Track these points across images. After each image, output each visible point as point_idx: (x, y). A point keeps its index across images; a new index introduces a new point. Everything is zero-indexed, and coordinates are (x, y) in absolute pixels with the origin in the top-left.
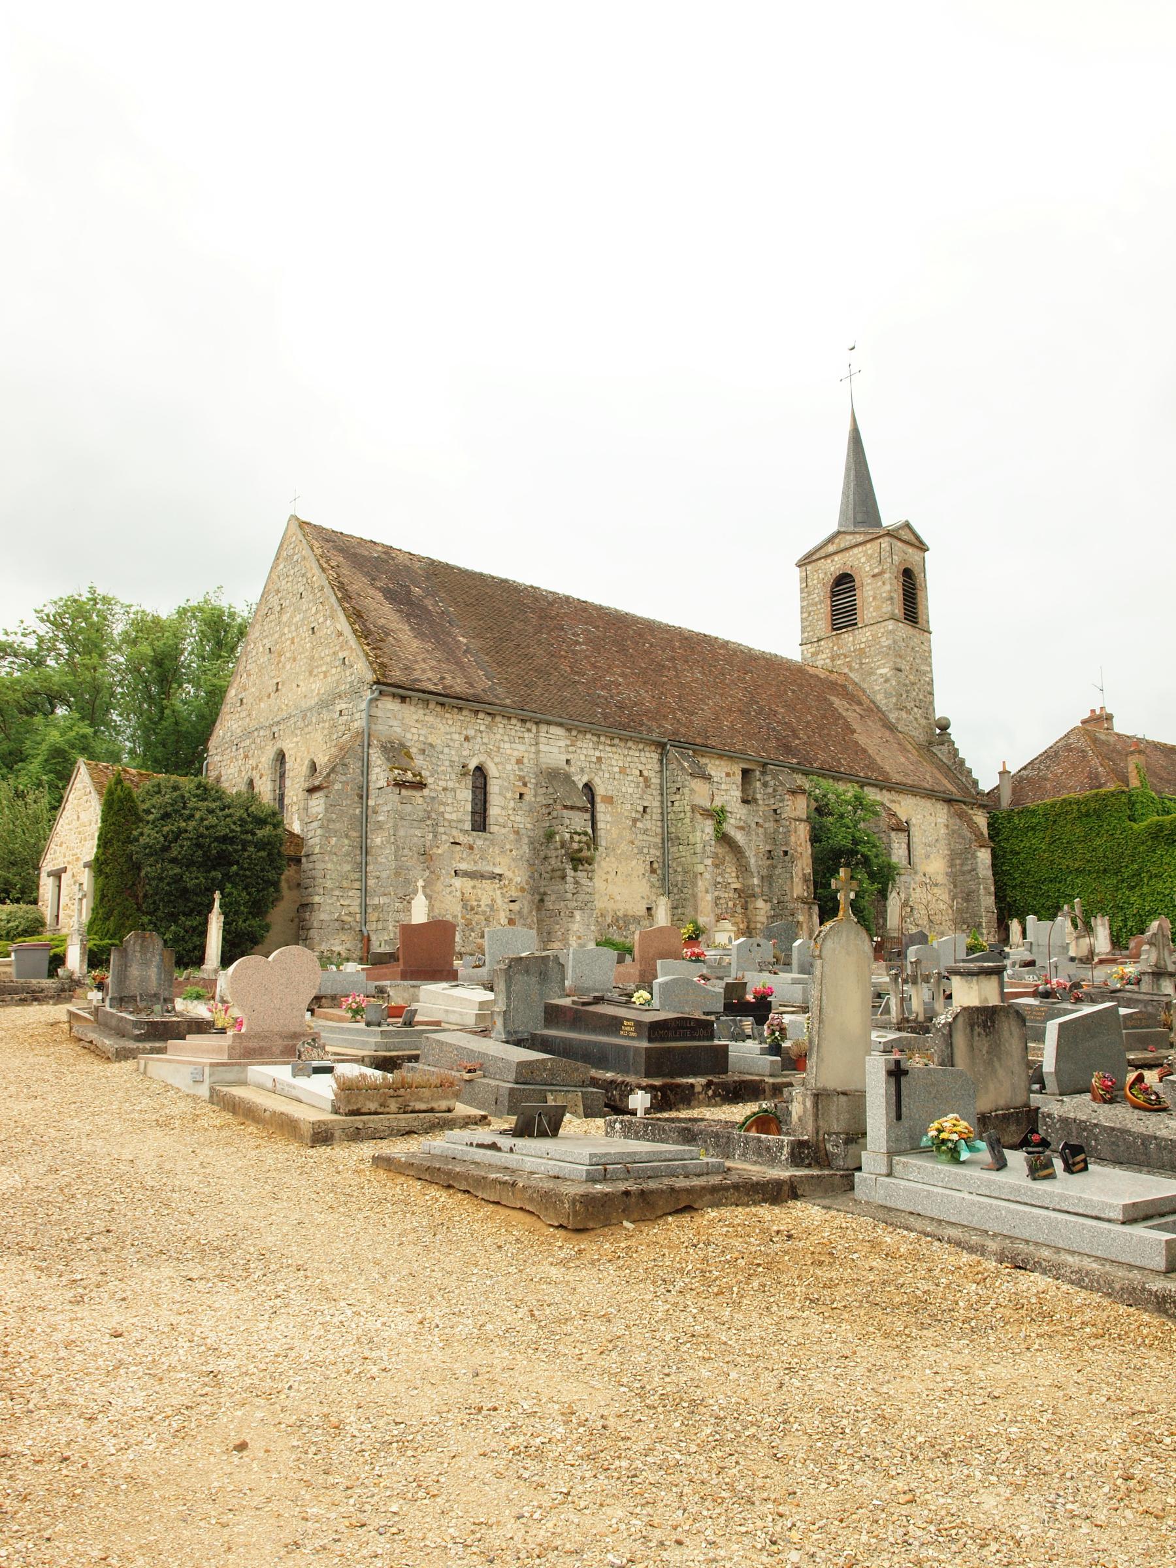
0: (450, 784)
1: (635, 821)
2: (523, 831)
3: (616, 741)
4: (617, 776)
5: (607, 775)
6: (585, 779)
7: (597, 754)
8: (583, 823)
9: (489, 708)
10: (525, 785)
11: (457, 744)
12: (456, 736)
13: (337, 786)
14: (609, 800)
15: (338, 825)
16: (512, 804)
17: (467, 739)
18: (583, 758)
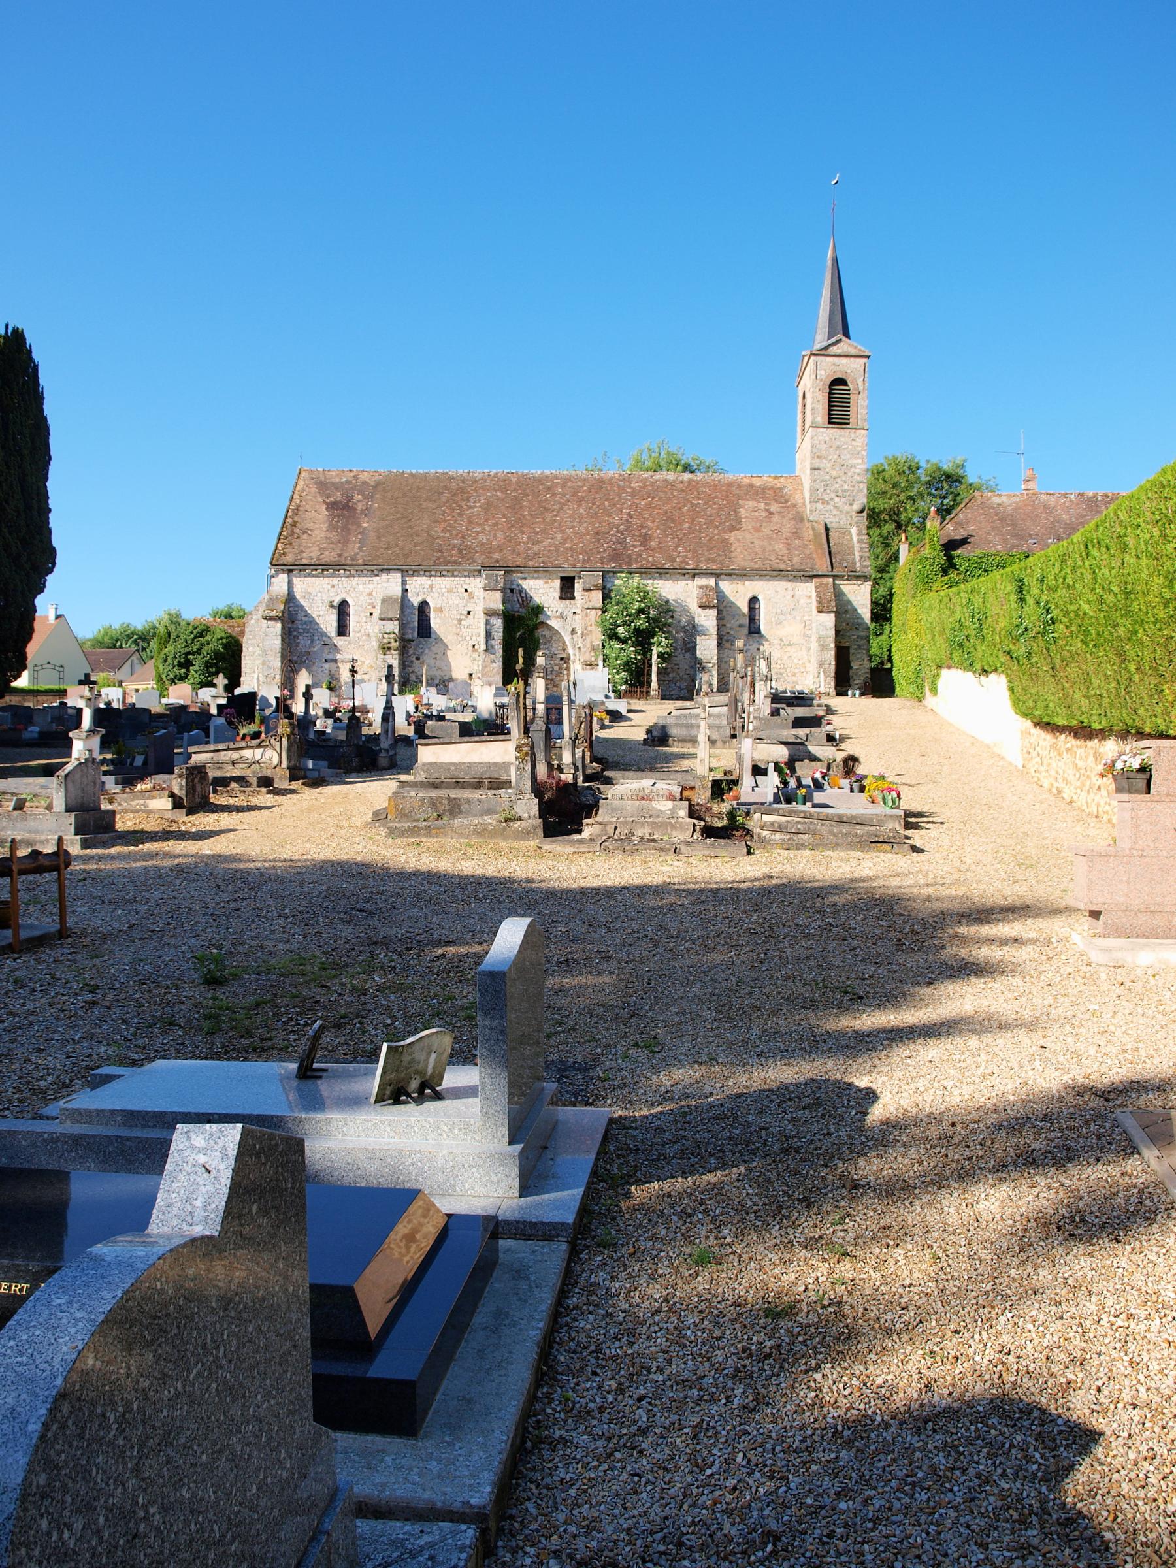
0: (322, 613)
1: (460, 621)
2: (371, 634)
3: (433, 573)
4: (445, 594)
5: (437, 595)
6: (420, 599)
7: (429, 583)
8: (392, 627)
9: (347, 568)
10: (374, 607)
11: (326, 590)
12: (325, 586)
13: (252, 622)
14: (440, 610)
15: (253, 641)
16: (364, 619)
17: (333, 586)
18: (417, 586)
